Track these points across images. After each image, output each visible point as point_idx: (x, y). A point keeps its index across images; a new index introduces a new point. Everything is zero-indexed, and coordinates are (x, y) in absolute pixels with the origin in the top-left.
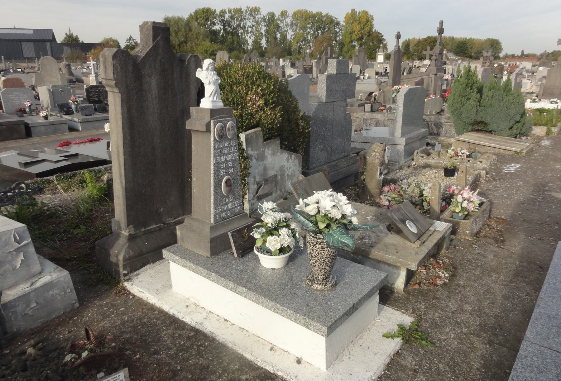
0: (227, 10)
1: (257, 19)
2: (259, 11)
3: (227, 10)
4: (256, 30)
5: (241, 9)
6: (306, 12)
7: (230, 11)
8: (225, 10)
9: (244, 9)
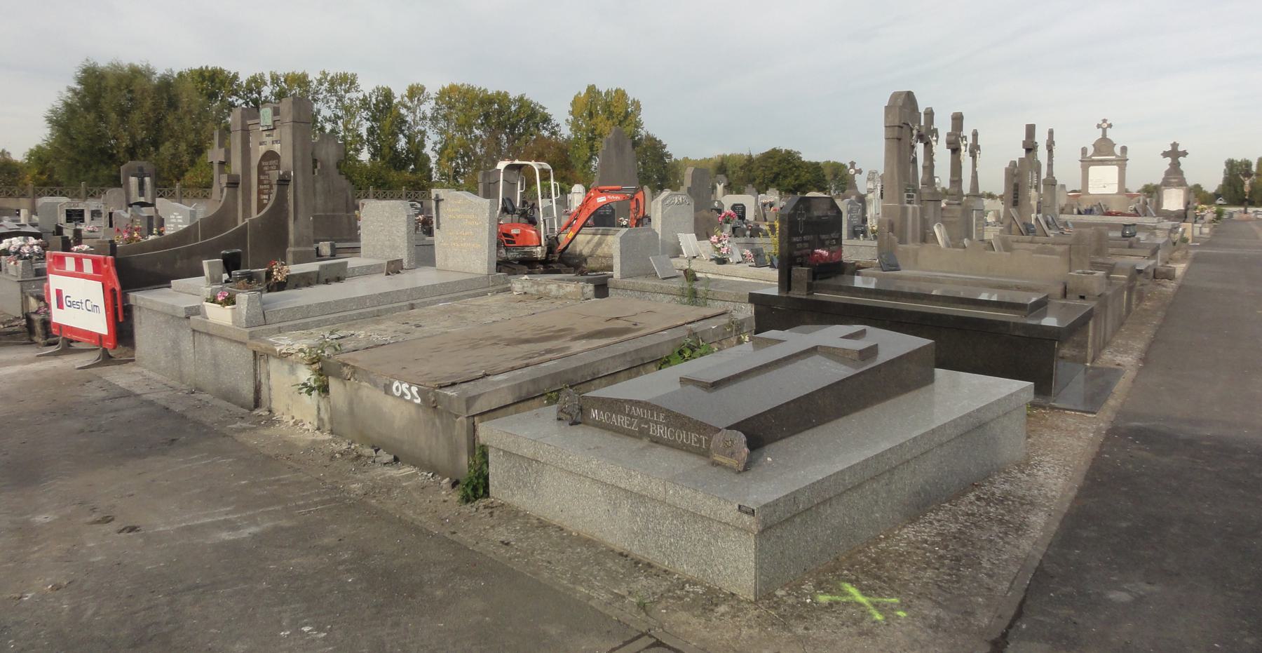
0: (268, 78)
1: (347, 102)
2: (352, 83)
3: (268, 78)
4: (346, 129)
5: (305, 76)
6: (470, 90)
7: (275, 80)
8: (262, 76)
9: (313, 76)
